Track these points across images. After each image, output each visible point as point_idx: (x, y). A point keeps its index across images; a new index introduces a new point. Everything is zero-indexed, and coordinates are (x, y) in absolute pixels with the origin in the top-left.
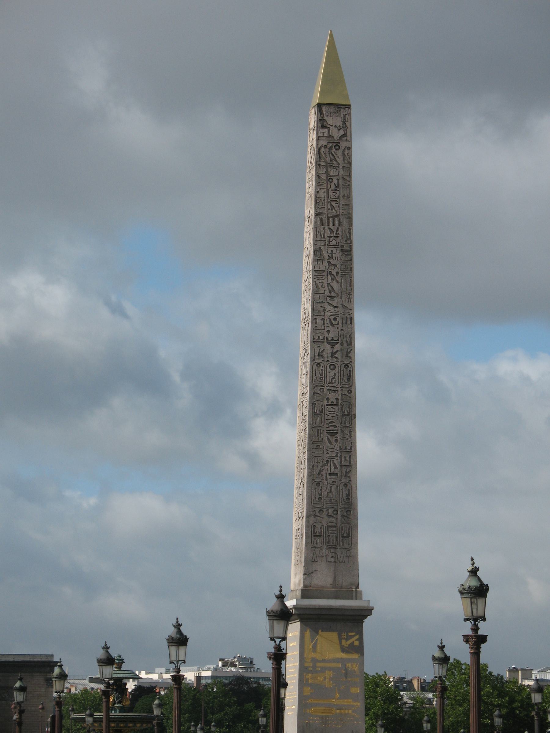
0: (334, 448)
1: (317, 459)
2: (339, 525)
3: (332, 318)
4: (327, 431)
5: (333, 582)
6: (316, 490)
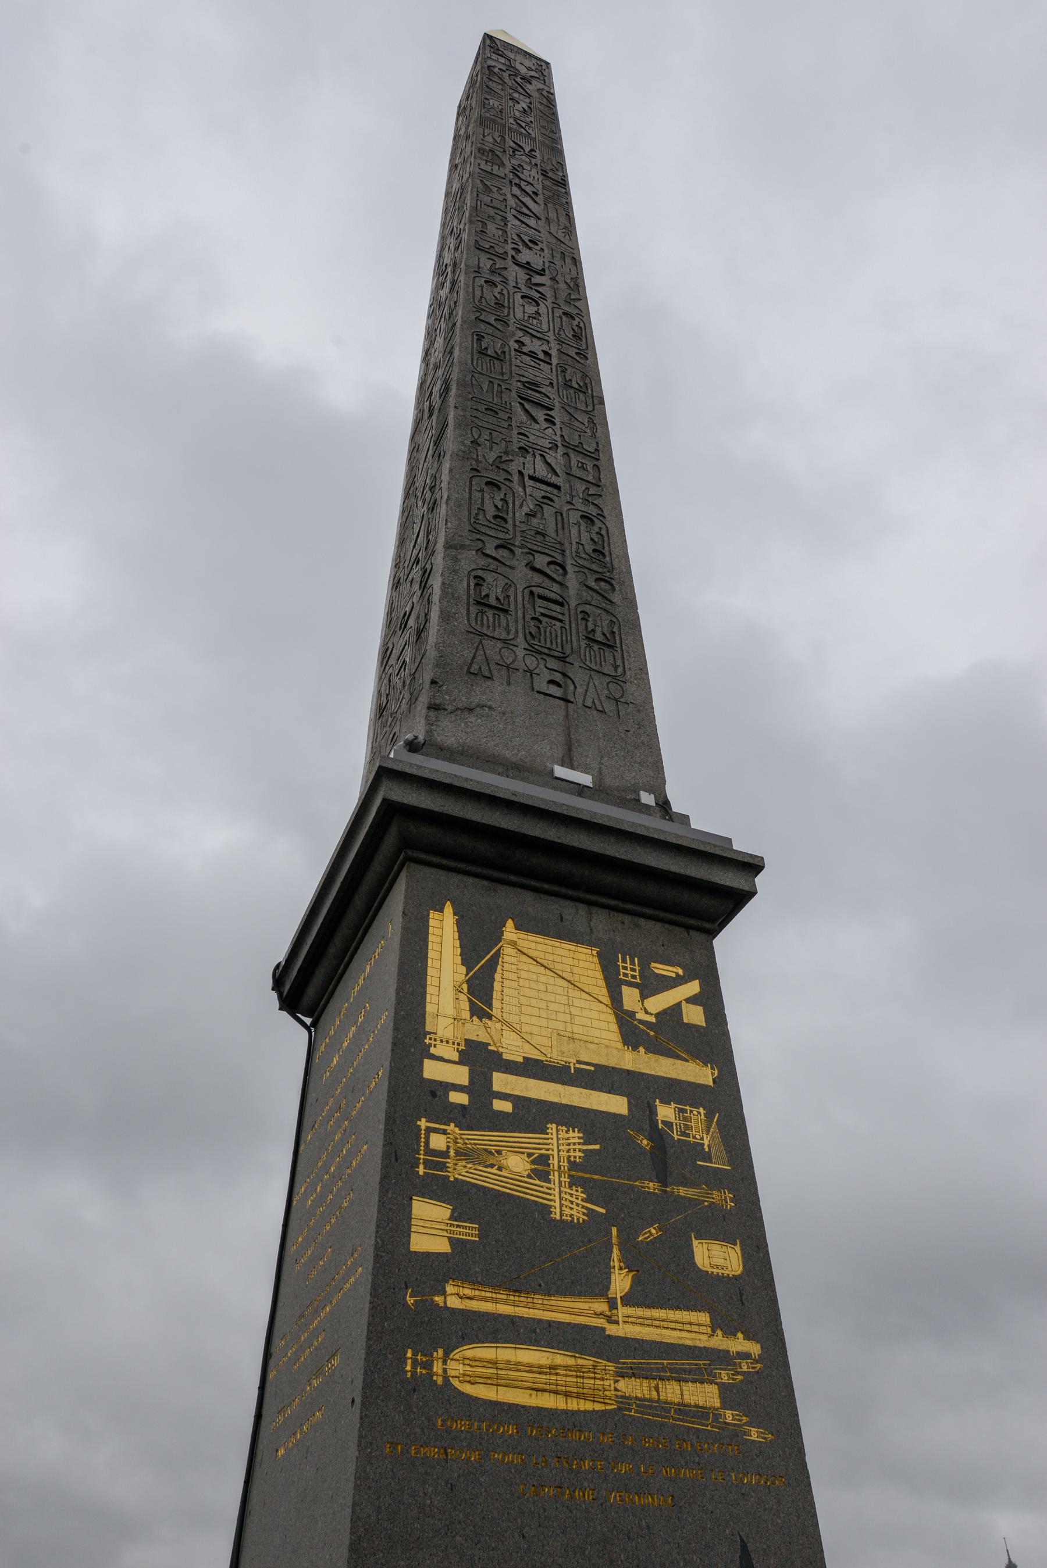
5: (563, 757)
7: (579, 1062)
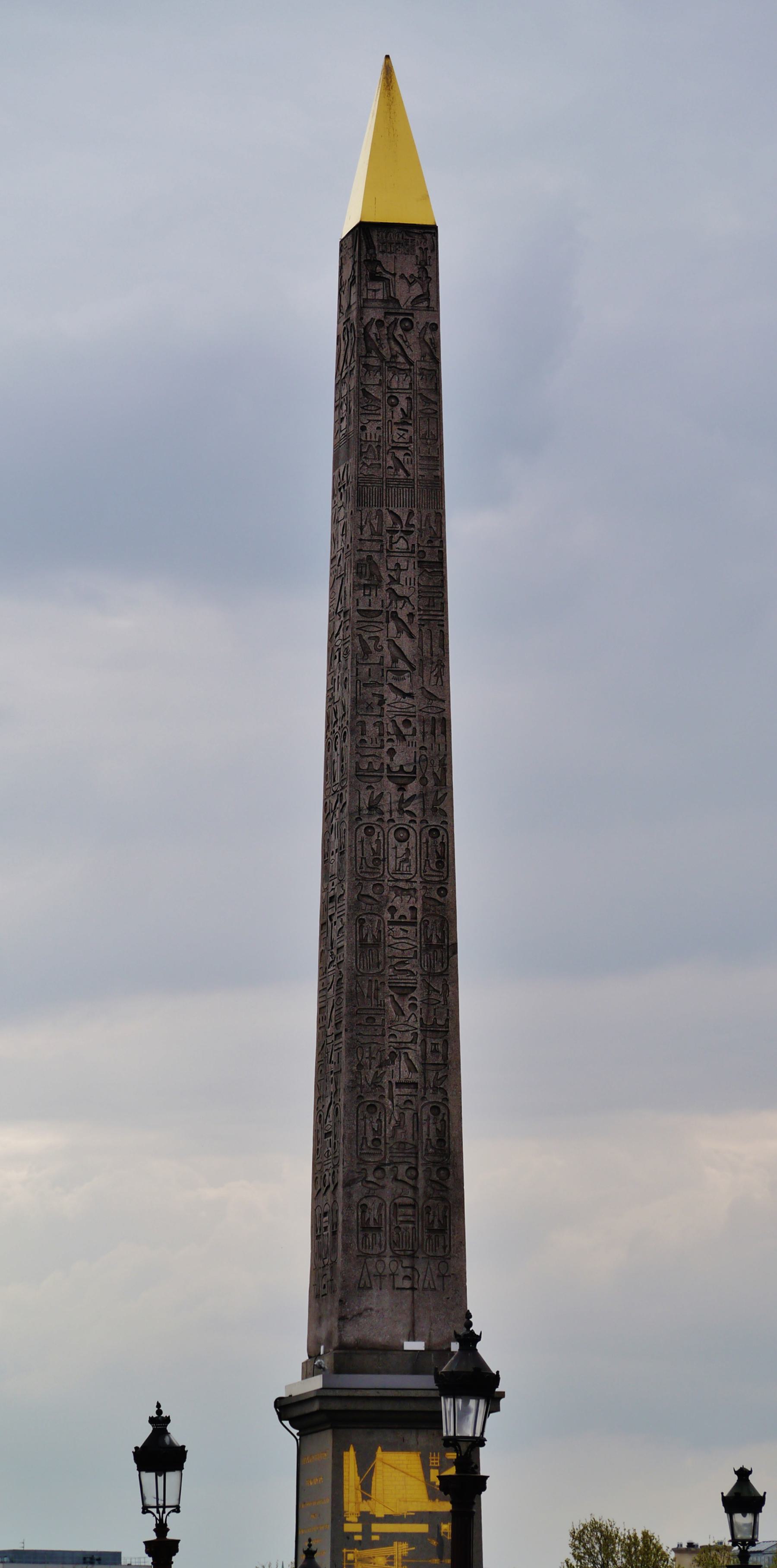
0: (406, 1023)
1: (367, 1049)
2: (420, 1203)
3: (399, 720)
4: (390, 985)
6: (368, 1122)
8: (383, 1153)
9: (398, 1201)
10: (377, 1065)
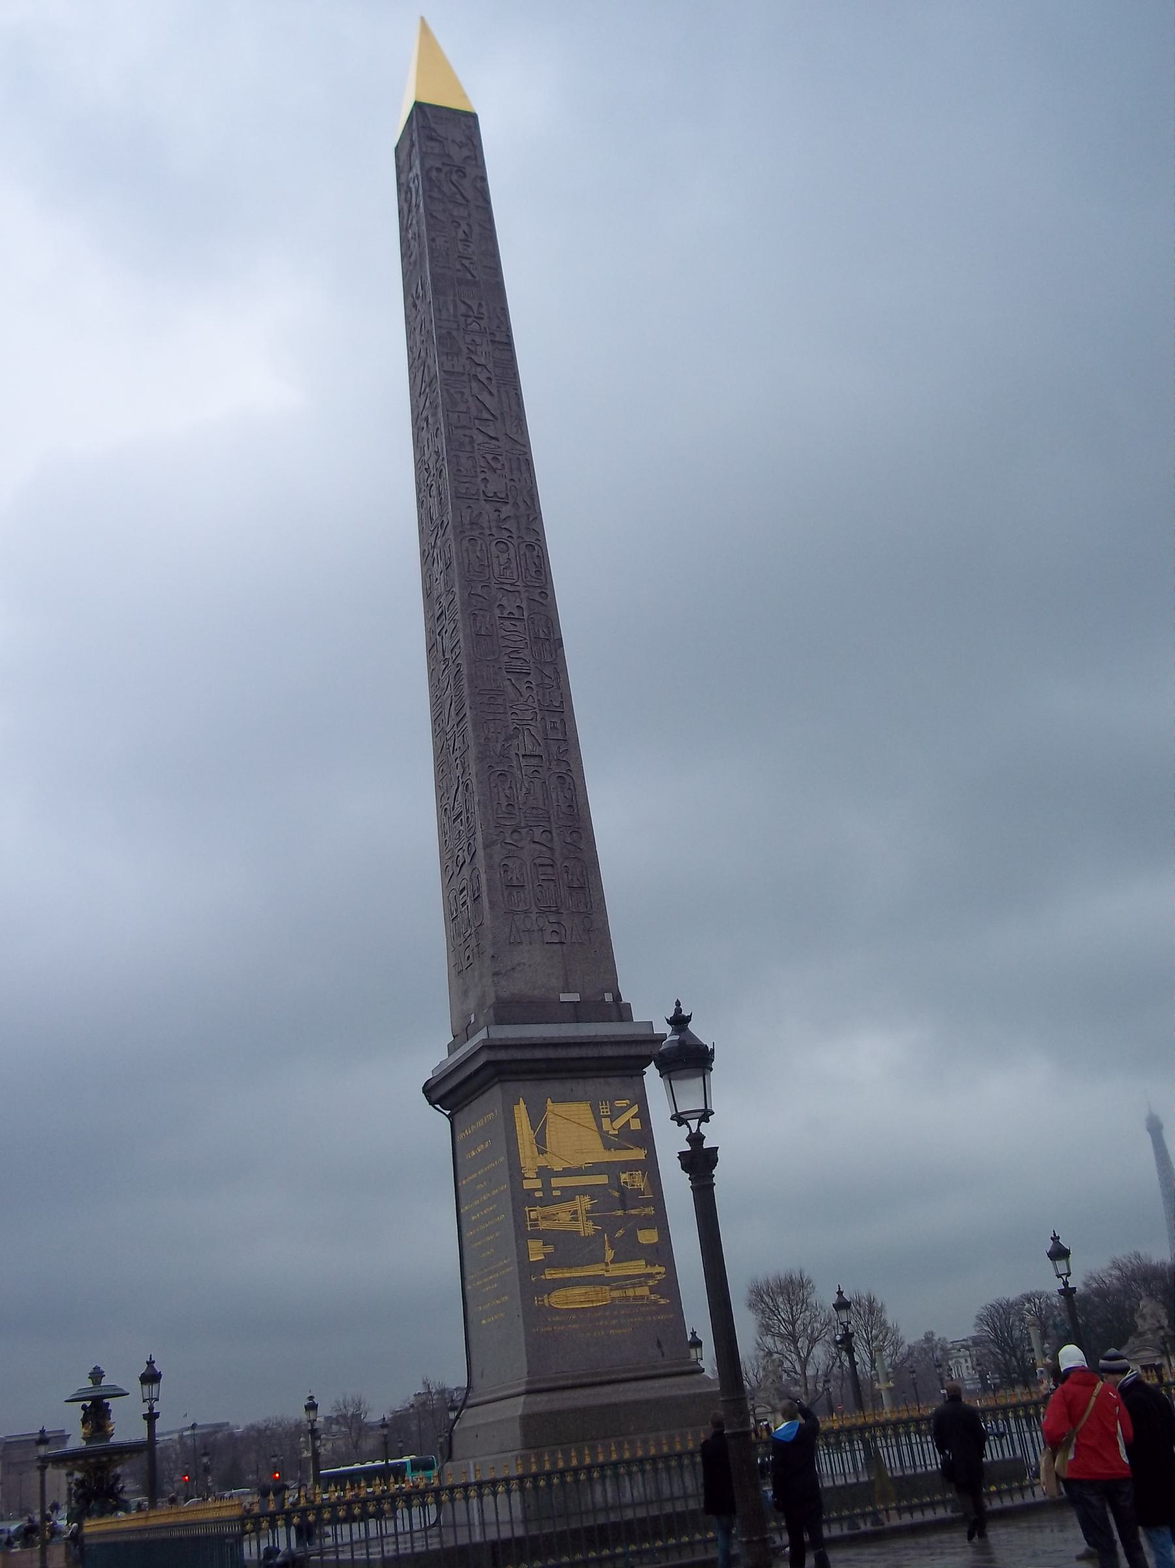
2: (559, 863)
7: (586, 1164)
8: (518, 817)
9: (538, 861)
10: (503, 739)
